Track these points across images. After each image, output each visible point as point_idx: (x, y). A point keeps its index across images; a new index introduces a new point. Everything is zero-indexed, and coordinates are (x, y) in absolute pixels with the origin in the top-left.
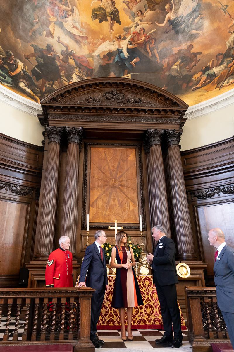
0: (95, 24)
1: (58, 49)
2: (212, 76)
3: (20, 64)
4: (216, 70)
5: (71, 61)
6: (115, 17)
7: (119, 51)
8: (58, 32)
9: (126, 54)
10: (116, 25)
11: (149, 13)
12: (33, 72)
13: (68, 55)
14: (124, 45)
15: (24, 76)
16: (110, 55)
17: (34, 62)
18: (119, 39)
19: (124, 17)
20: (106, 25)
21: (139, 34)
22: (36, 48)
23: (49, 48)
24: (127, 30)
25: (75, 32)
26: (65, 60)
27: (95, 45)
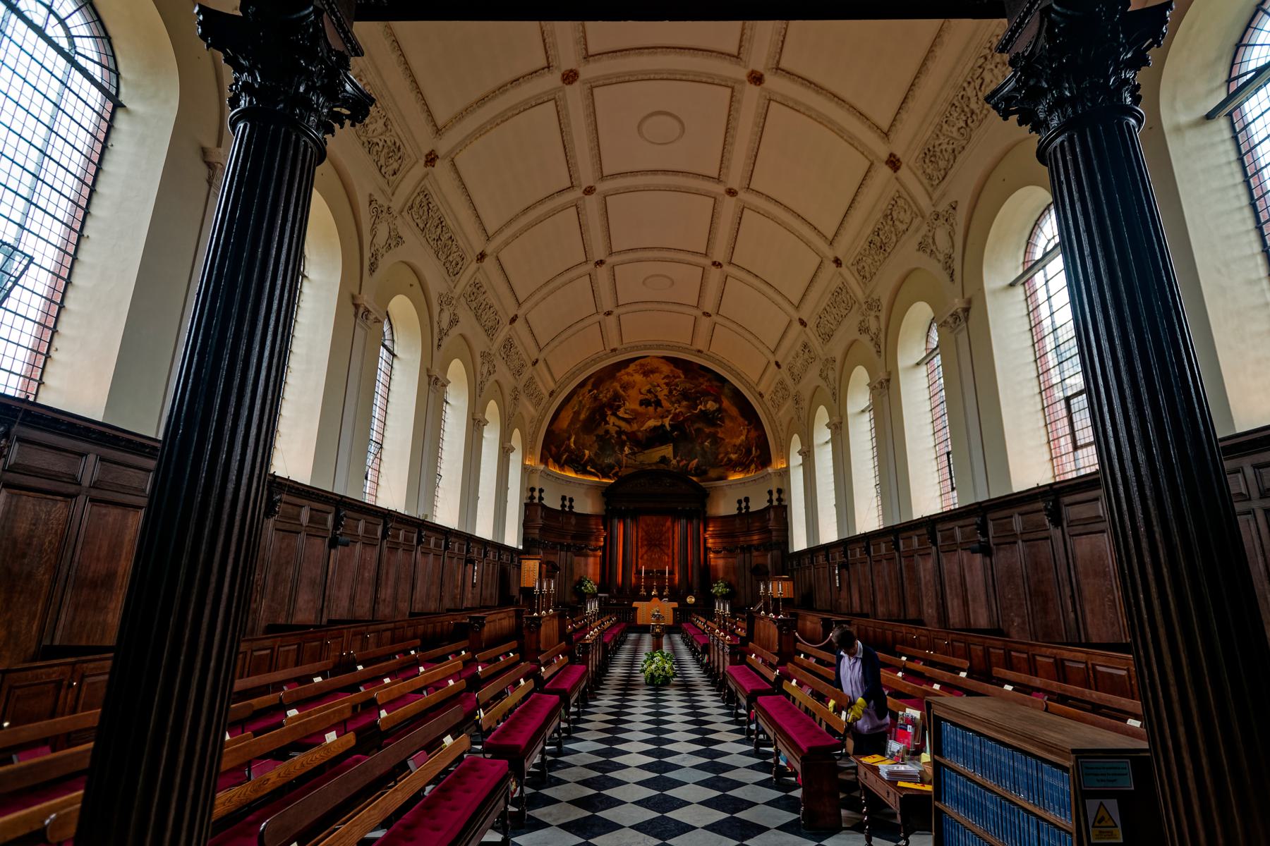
0: (641, 409)
1: (613, 430)
2: (730, 460)
3: (587, 452)
4: (733, 456)
5: (624, 437)
6: (658, 403)
7: (663, 426)
8: (611, 419)
9: (668, 428)
10: (659, 409)
11: (685, 403)
12: (596, 454)
13: (620, 432)
14: (667, 422)
15: (590, 460)
16: (656, 428)
17: (596, 446)
18: (662, 417)
19: (666, 404)
20: (651, 409)
21: (676, 416)
22: (597, 436)
23: (607, 432)
24: (669, 412)
25: (626, 416)
26: (619, 437)
27: (644, 423)
